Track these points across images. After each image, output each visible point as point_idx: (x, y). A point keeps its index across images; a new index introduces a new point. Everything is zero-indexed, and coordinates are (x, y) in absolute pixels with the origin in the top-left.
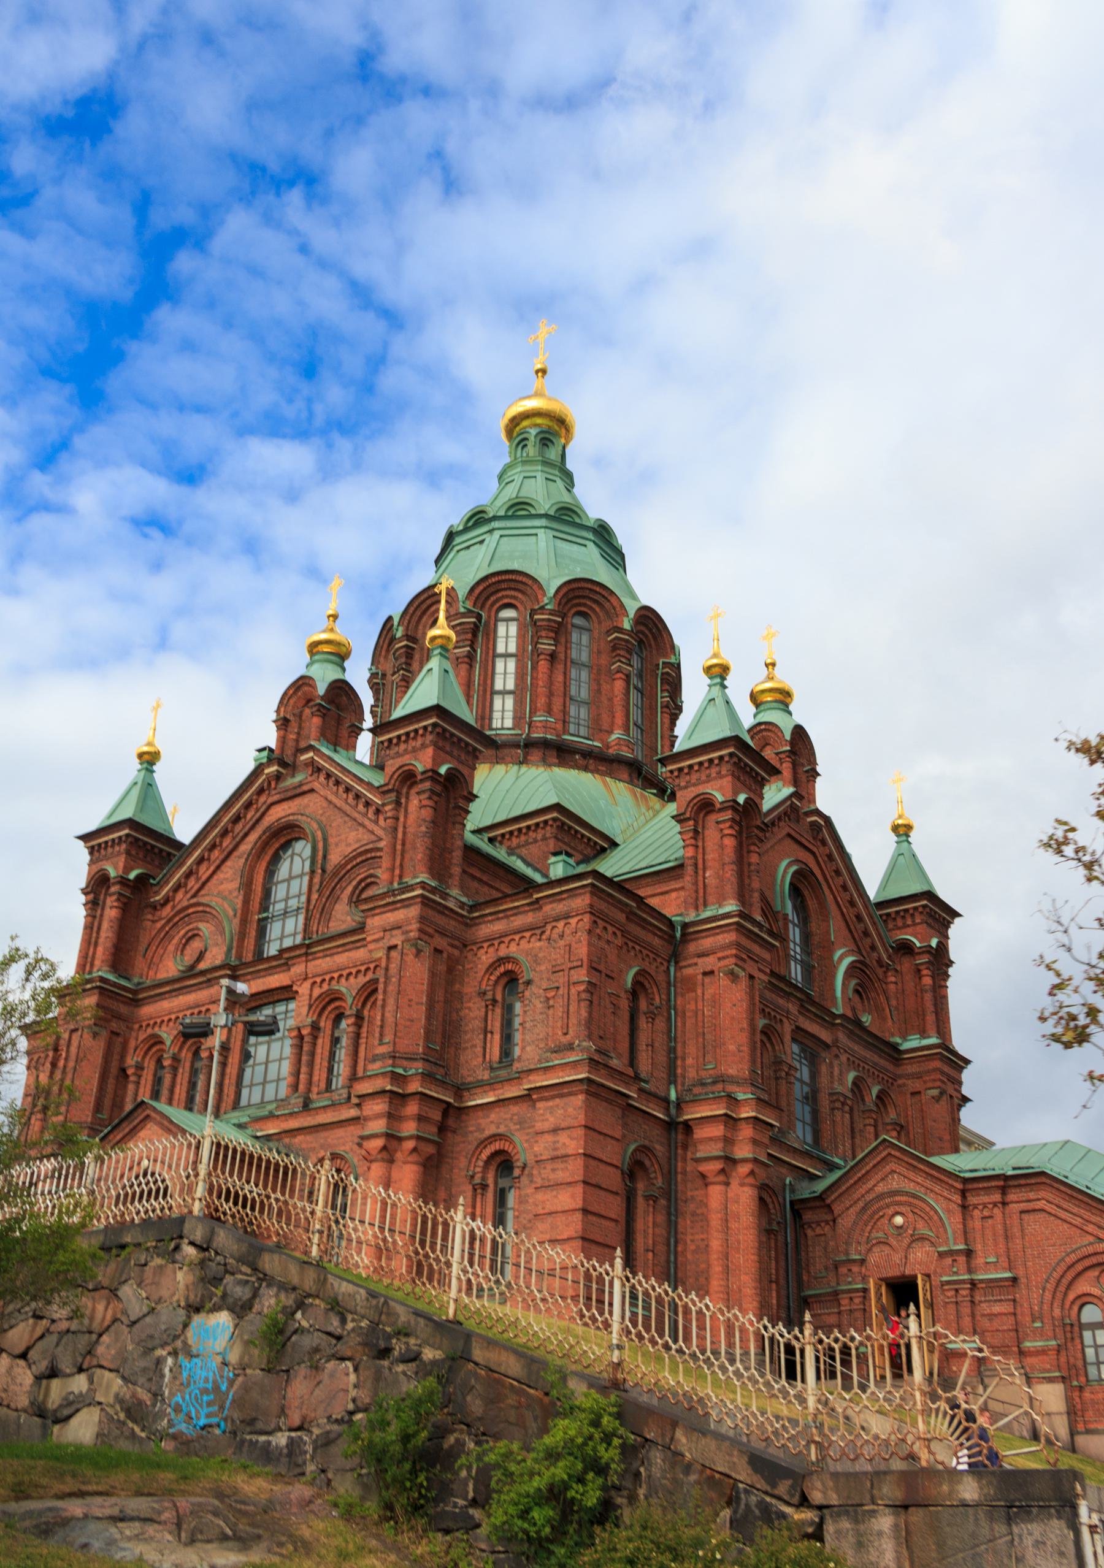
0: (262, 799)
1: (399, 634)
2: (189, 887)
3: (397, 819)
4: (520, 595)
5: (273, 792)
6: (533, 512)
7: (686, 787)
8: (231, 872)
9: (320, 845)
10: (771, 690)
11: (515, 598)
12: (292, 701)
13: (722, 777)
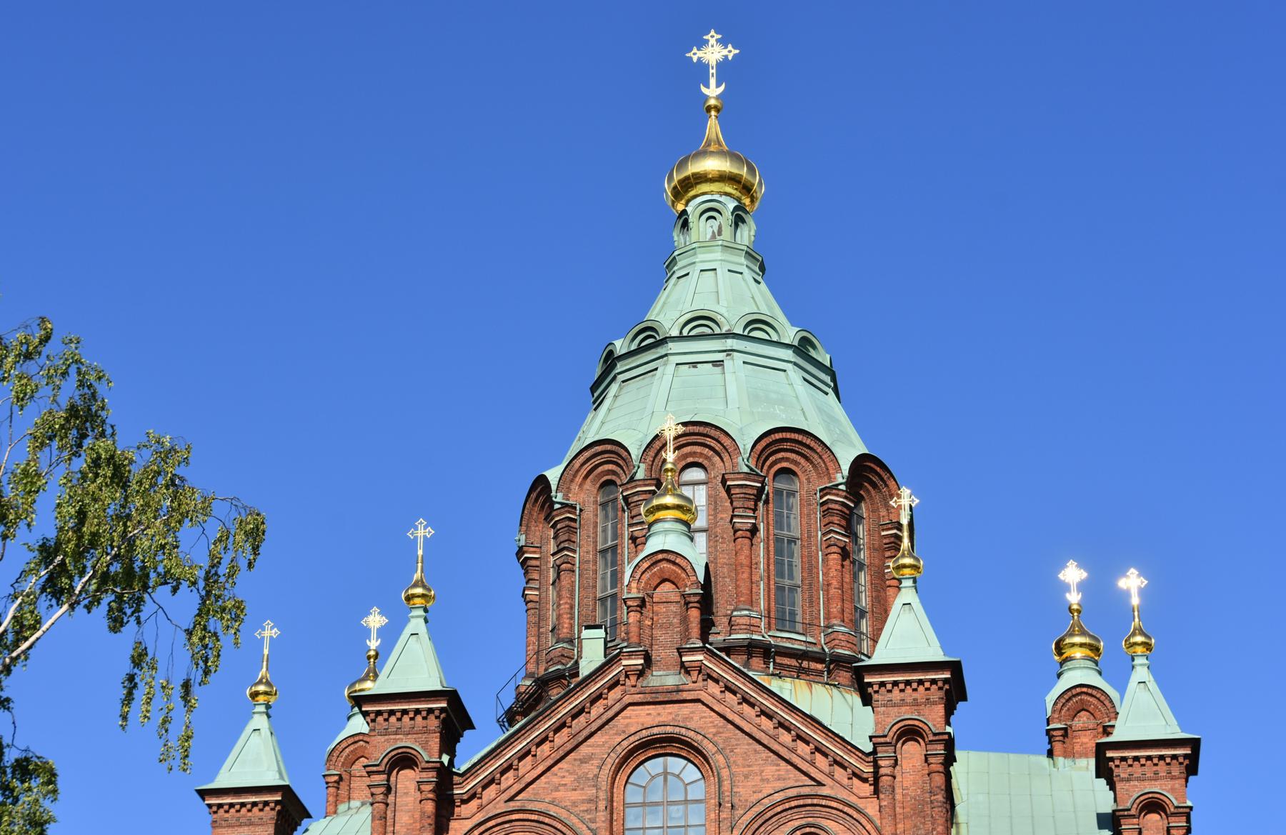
0: (615, 694)
1: (640, 475)
2: (503, 786)
3: (894, 777)
4: (802, 461)
5: (633, 690)
6: (775, 338)
7: (1128, 780)
8: (569, 779)
9: (725, 773)
10: (1082, 645)
11: (797, 464)
12: (647, 575)
13: (1173, 778)
